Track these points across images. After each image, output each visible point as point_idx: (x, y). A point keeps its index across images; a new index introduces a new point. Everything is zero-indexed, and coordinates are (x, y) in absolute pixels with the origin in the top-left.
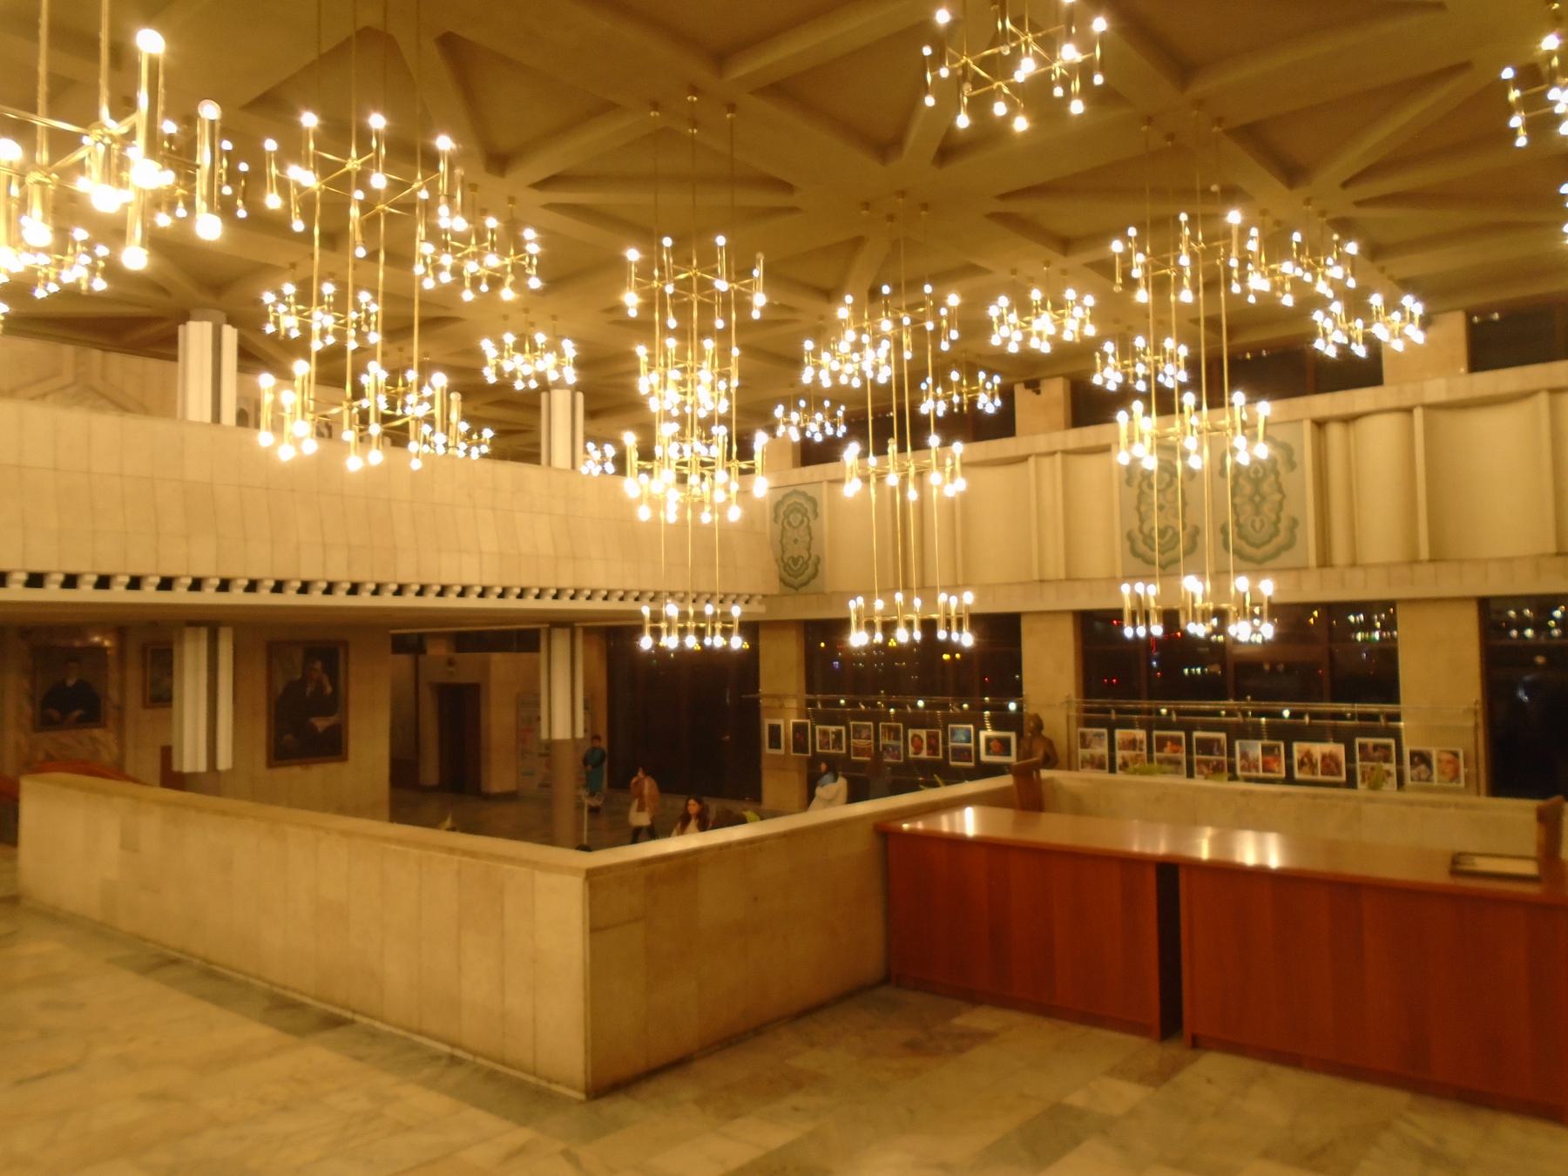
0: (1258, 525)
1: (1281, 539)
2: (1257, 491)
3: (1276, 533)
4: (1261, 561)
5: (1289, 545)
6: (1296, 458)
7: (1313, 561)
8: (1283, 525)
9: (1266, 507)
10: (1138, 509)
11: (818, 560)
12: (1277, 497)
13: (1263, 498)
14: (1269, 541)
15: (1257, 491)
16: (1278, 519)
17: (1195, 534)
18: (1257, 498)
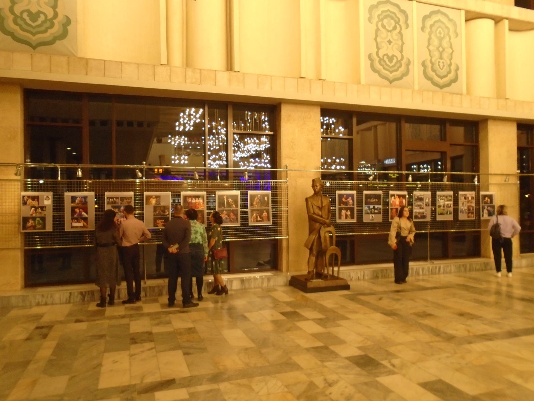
1: (451, 76)
2: (440, 45)
3: (449, 72)
4: (442, 87)
5: (455, 80)
6: (458, 31)
7: (465, 91)
8: (453, 67)
9: (445, 55)
10: (376, 39)
11: (68, 22)
12: (451, 51)
13: (444, 50)
15: (440, 45)
16: (450, 65)
17: (409, 63)
18: (441, 49)
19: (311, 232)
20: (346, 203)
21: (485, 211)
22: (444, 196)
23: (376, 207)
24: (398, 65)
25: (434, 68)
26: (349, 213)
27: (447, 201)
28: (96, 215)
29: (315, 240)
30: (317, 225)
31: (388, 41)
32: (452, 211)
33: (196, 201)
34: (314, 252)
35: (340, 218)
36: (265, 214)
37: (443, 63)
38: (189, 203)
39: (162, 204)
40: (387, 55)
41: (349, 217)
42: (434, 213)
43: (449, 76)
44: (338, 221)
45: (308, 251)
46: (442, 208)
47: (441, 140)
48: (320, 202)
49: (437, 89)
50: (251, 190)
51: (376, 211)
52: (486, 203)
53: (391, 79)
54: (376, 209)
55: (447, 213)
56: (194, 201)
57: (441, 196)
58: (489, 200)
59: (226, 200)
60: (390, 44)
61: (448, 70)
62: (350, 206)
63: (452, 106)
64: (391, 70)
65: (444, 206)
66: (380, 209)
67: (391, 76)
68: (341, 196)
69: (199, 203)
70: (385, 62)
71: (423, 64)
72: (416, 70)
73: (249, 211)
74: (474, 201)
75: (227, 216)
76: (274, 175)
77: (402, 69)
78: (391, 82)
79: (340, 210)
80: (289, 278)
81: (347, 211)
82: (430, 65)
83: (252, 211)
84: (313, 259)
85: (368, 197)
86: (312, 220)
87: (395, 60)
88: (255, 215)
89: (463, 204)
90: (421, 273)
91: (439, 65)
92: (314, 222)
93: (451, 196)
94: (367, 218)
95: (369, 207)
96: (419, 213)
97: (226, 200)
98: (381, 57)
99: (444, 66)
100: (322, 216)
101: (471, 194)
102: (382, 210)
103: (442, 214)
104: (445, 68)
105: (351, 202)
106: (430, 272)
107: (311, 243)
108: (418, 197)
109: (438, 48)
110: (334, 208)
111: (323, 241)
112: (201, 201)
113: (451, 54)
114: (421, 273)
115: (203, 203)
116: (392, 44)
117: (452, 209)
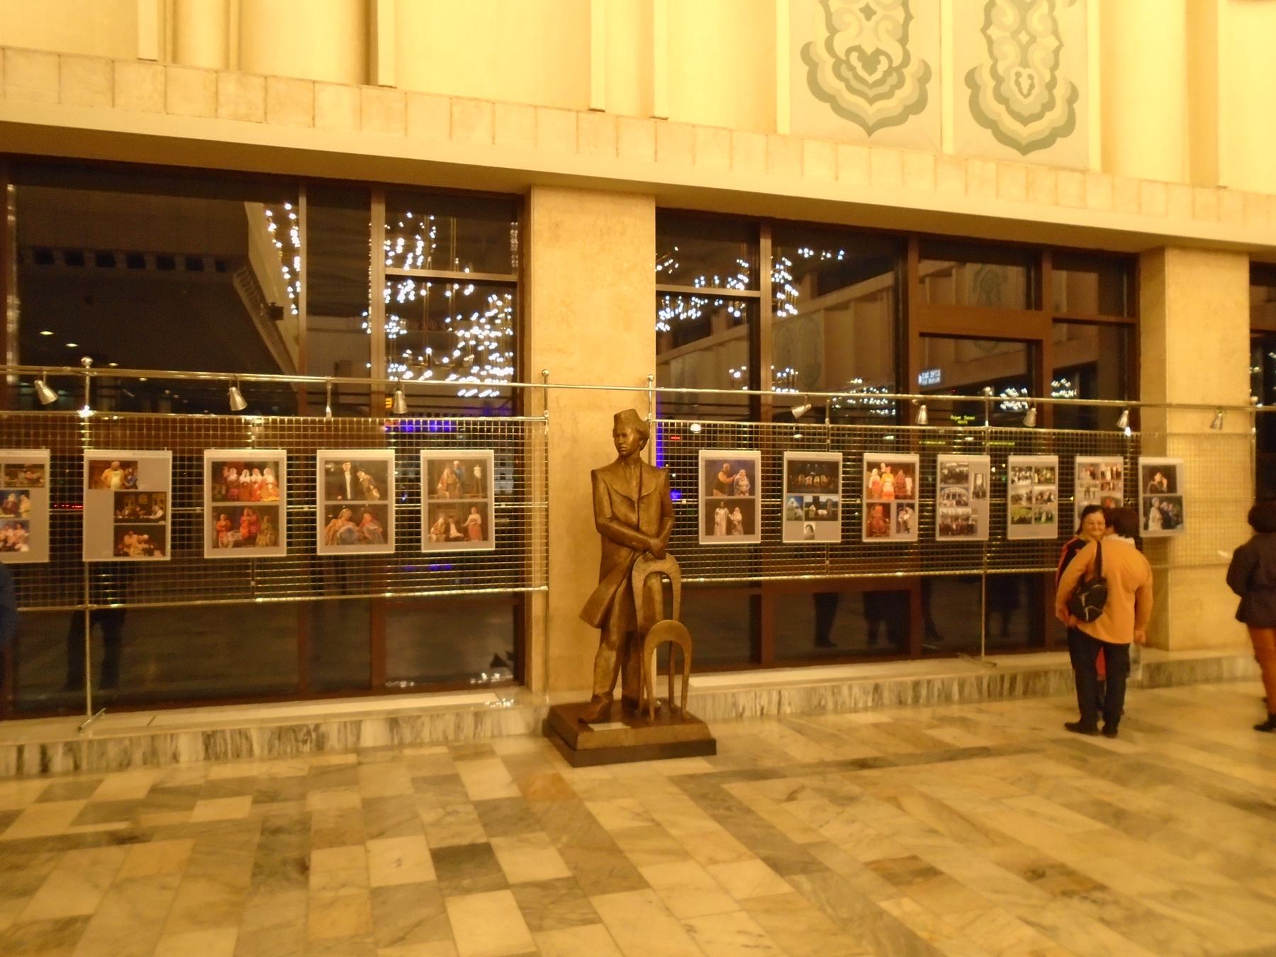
0: (1025, 83)
1: (1055, 116)
2: (1023, 24)
3: (1049, 105)
4: (1025, 149)
5: (1068, 127)
7: (1095, 163)
8: (1060, 92)
9: (1038, 55)
12: (1053, 43)
13: (1033, 39)
14: (1038, 117)
16: (1051, 85)
18: (1024, 37)
19: (607, 570)
20: (731, 488)
21: (1154, 514)
22: (1030, 469)
23: (823, 498)
24: (893, 79)
25: (1004, 89)
26: (737, 516)
27: (1040, 482)
28: (52, 518)
29: (617, 600)
30: (624, 553)
31: (862, 10)
32: (1055, 513)
33: (254, 478)
34: (615, 637)
35: (710, 531)
36: (474, 517)
37: (1031, 77)
38: (229, 486)
39: (142, 487)
40: (858, 49)
41: (740, 527)
42: (999, 518)
43: (1048, 115)
44: (704, 540)
45: (597, 633)
46: (1024, 503)
47: (1028, 306)
48: (634, 483)
49: (1015, 153)
50: (330, 446)
51: (822, 512)
52: (1155, 490)
53: (871, 123)
54: (823, 506)
55: (1038, 519)
56: (245, 478)
57: (1021, 470)
58: (1165, 482)
59: (348, 477)
60: (868, 18)
61: (1045, 99)
62: (742, 497)
63: (1056, 204)
64: (871, 93)
65: (1029, 499)
66: (835, 504)
67: (872, 112)
68: (712, 465)
69: (263, 485)
70: (853, 69)
71: (971, 80)
72: (948, 96)
73: (423, 507)
74: (1121, 484)
75: (351, 525)
76: (515, 401)
77: (907, 92)
78: (870, 131)
79: (712, 506)
80: (544, 714)
81: (732, 512)
82: (988, 83)
83: (434, 510)
84: (612, 656)
85: (799, 468)
86: (611, 539)
87: (883, 65)
88: (441, 521)
89: (1088, 491)
90: (956, 696)
91: (1018, 84)
92: (614, 546)
93: (1052, 469)
94: (795, 533)
95: (800, 500)
96: (956, 518)
97: (348, 477)
98: (843, 57)
99: (1032, 87)
100: (637, 528)
101: (1110, 463)
102: (840, 509)
103: (1023, 521)
104: (1035, 92)
105: (744, 483)
106: (985, 694)
107: (603, 608)
108: (951, 470)
109: (1015, 34)
110: (691, 502)
111: (639, 601)
112: (270, 478)
113: (1056, 52)
114: (956, 696)
115: (277, 484)
116: (874, 18)
117: (1053, 507)
